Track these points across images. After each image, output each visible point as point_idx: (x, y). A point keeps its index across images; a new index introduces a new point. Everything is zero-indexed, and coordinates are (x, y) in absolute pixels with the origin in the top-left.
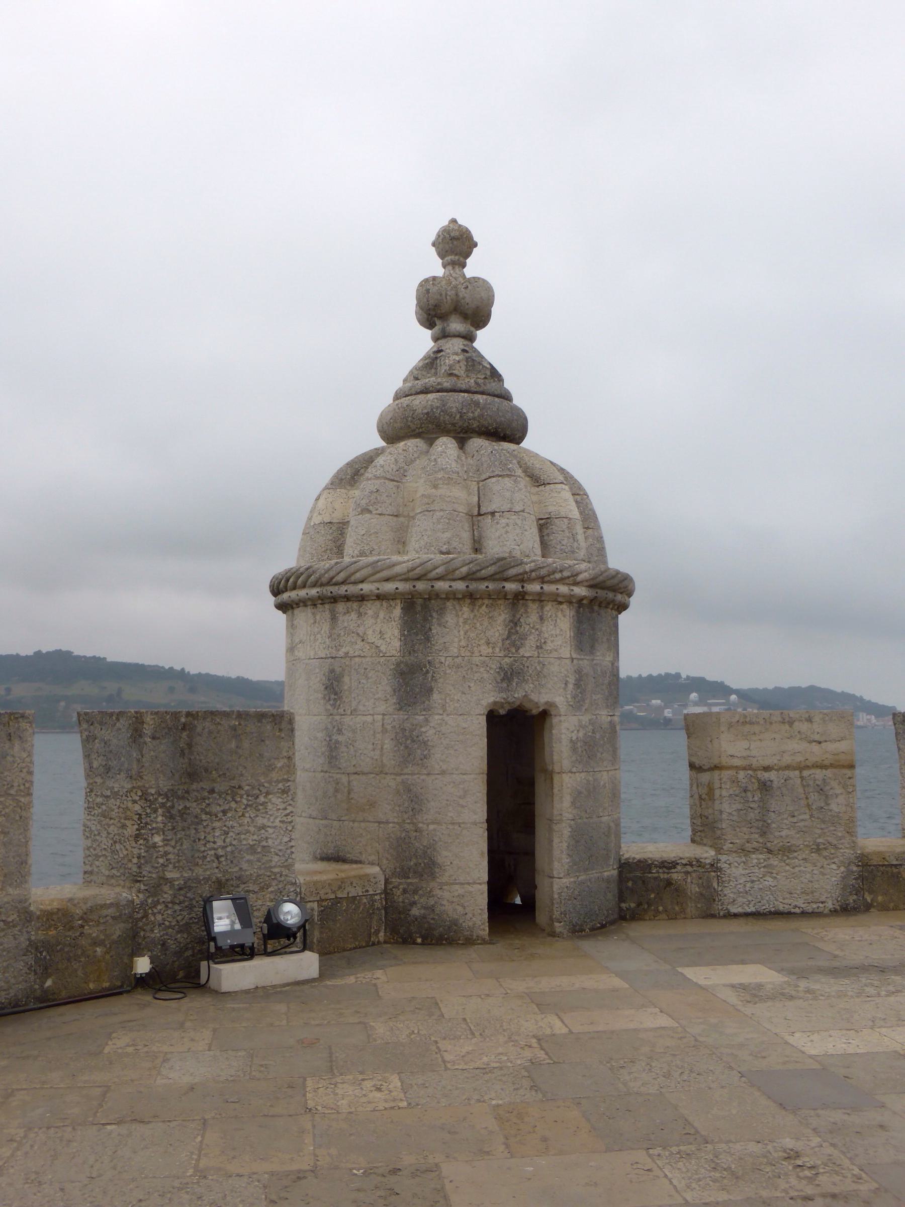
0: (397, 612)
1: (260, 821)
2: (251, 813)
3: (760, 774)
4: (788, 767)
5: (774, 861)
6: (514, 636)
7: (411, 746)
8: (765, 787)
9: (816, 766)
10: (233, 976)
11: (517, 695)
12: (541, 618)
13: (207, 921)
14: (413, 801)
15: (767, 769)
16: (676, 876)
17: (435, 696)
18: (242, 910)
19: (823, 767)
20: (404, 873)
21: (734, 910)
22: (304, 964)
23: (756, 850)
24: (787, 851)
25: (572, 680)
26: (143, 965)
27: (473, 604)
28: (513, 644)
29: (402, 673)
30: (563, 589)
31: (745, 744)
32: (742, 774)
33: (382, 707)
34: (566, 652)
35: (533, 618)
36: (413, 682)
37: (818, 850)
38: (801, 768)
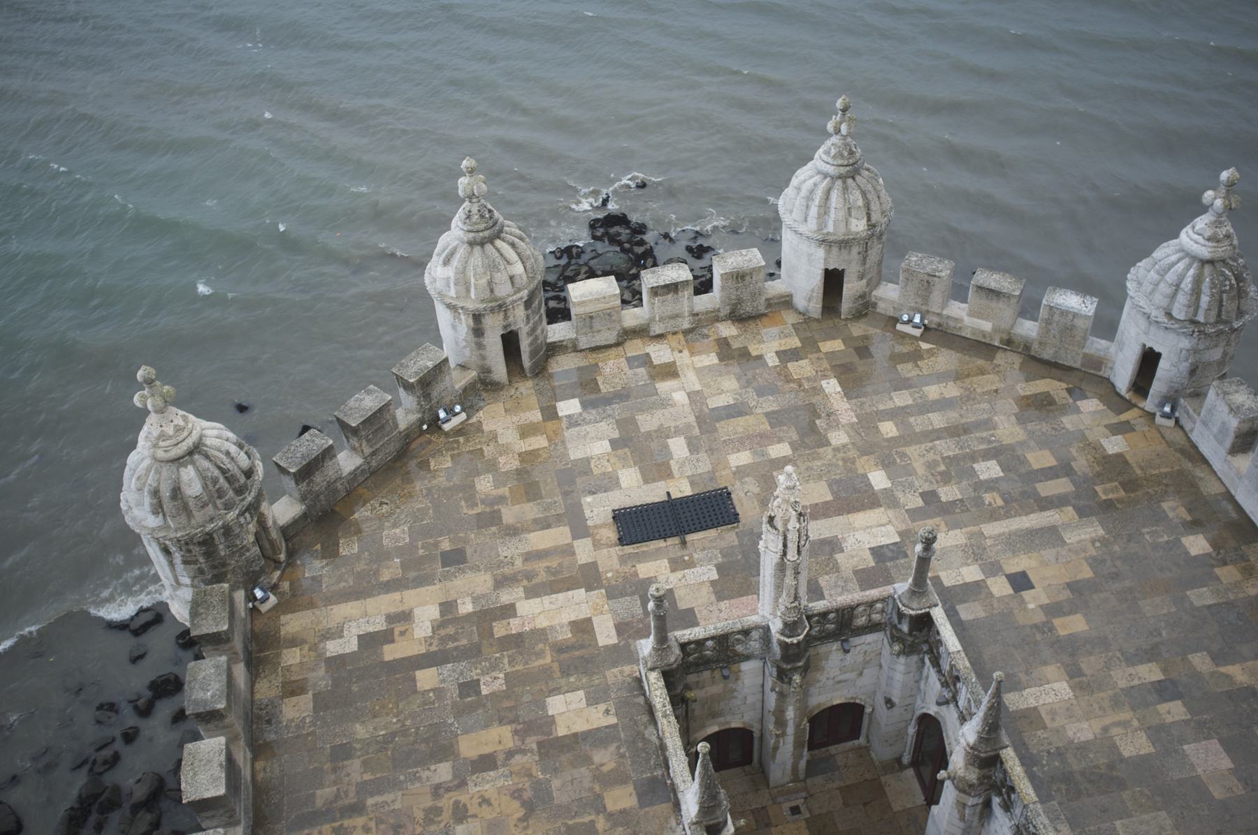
10: (447, 427)
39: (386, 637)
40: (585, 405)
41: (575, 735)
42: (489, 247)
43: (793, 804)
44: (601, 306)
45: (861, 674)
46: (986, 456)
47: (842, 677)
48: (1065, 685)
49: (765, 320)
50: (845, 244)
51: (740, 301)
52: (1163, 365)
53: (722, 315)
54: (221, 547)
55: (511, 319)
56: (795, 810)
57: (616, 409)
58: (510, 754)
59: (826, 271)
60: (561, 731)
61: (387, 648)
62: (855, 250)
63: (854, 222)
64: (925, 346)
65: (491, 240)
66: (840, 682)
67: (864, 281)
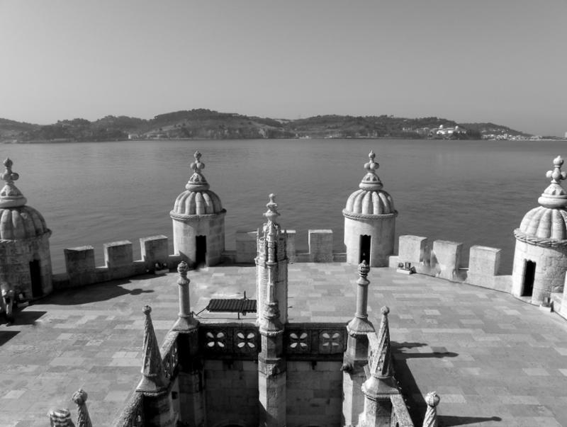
10: (157, 272)
11: (200, 234)
26: (148, 271)
39: (62, 322)
40: (226, 275)
41: (117, 367)
45: (328, 402)
46: (431, 308)
48: (462, 397)
52: (538, 269)
54: (8, 258)
57: (239, 278)
58: (74, 368)
59: (361, 236)
60: (111, 365)
61: (58, 324)
66: (314, 405)
67: (381, 246)
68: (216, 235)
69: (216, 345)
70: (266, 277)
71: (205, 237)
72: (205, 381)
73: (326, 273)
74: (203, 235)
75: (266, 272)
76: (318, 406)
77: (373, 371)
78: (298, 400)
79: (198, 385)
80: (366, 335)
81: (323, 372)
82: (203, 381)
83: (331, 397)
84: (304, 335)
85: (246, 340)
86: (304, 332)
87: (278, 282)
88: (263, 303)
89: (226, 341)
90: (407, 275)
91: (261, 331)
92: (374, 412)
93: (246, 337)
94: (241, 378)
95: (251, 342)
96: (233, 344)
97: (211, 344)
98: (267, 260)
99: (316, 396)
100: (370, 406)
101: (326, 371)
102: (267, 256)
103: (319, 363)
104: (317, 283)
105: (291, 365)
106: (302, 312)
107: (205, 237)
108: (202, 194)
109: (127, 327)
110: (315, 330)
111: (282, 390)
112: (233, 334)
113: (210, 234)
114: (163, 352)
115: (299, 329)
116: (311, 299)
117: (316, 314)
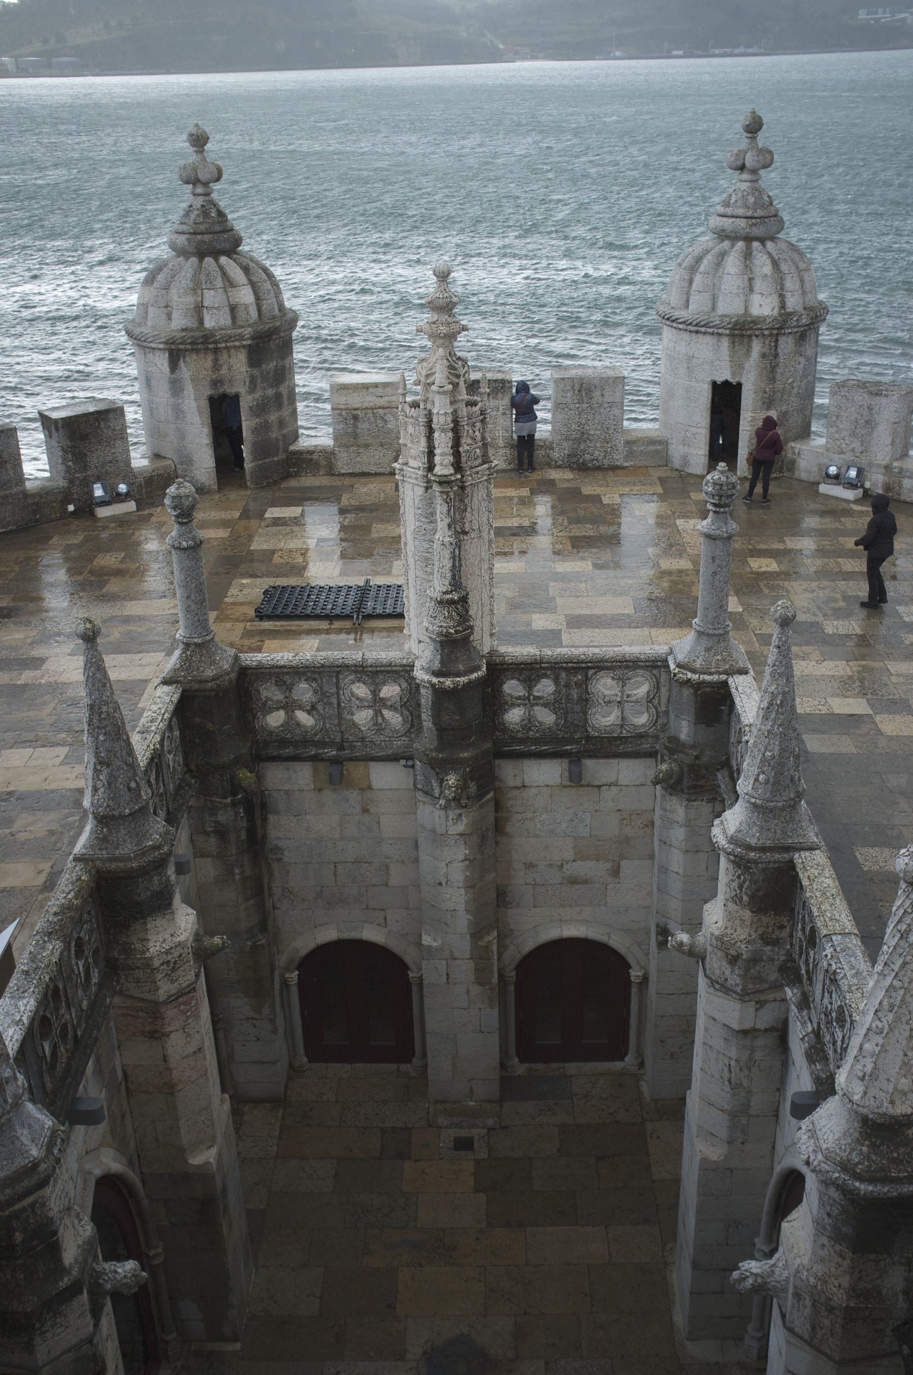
0: (167, 355)
1: (113, 451)
2: (108, 448)
3: (353, 412)
4: (367, 408)
5: (361, 450)
6: (216, 366)
7: (178, 412)
8: (356, 418)
9: (379, 408)
10: (103, 512)
12: (229, 357)
13: (91, 491)
14: (182, 436)
15: (356, 409)
16: (315, 457)
17: (185, 392)
18: (104, 488)
19: (383, 408)
20: (182, 463)
21: (342, 471)
22: (131, 506)
23: (352, 446)
24: (367, 446)
25: (248, 381)
26: (71, 508)
27: (197, 353)
28: (217, 369)
29: (172, 382)
30: (237, 344)
31: (345, 398)
32: (344, 413)
33: (166, 396)
34: (243, 369)
35: (225, 356)
36: (176, 387)
37: (382, 446)
38: (372, 409)
42: (209, 260)
43: (464, 1133)
44: (369, 400)
45: (616, 872)
47: (581, 868)
49: (619, 472)
50: (741, 331)
51: (583, 437)
53: (556, 455)
55: (224, 371)
56: (464, 1145)
59: (714, 384)
62: (757, 347)
63: (756, 299)
64: (855, 507)
65: (216, 254)
66: (573, 881)
68: (270, 392)
69: (290, 717)
70: (430, 517)
71: (236, 397)
72: (265, 820)
73: (605, 501)
74: (232, 391)
75: (430, 503)
76: (586, 882)
77: (744, 786)
78: (530, 866)
79: (243, 835)
80: (725, 684)
81: (599, 787)
82: (258, 823)
83: (622, 857)
84: (545, 687)
85: (378, 703)
86: (545, 676)
87: (465, 533)
88: (421, 593)
89: (320, 707)
90: (847, 501)
91: (420, 675)
92: (745, 898)
93: (375, 693)
94: (365, 811)
95: (392, 708)
96: (340, 716)
97: (275, 719)
98: (431, 467)
99: (580, 856)
100: (735, 885)
101: (610, 785)
102: (431, 454)
103: (589, 763)
104: (577, 531)
105: (508, 772)
106: (535, 617)
107: (236, 397)
108: (217, 260)
109: (27, 676)
110: (576, 670)
111: (483, 837)
112: (338, 688)
113: (252, 389)
114: (142, 746)
115: (530, 671)
116: (562, 578)
117: (577, 622)
